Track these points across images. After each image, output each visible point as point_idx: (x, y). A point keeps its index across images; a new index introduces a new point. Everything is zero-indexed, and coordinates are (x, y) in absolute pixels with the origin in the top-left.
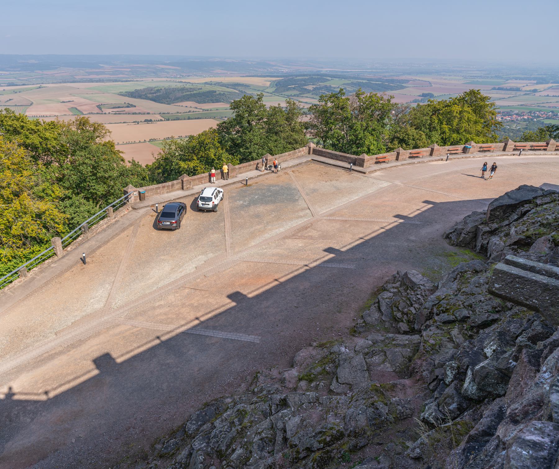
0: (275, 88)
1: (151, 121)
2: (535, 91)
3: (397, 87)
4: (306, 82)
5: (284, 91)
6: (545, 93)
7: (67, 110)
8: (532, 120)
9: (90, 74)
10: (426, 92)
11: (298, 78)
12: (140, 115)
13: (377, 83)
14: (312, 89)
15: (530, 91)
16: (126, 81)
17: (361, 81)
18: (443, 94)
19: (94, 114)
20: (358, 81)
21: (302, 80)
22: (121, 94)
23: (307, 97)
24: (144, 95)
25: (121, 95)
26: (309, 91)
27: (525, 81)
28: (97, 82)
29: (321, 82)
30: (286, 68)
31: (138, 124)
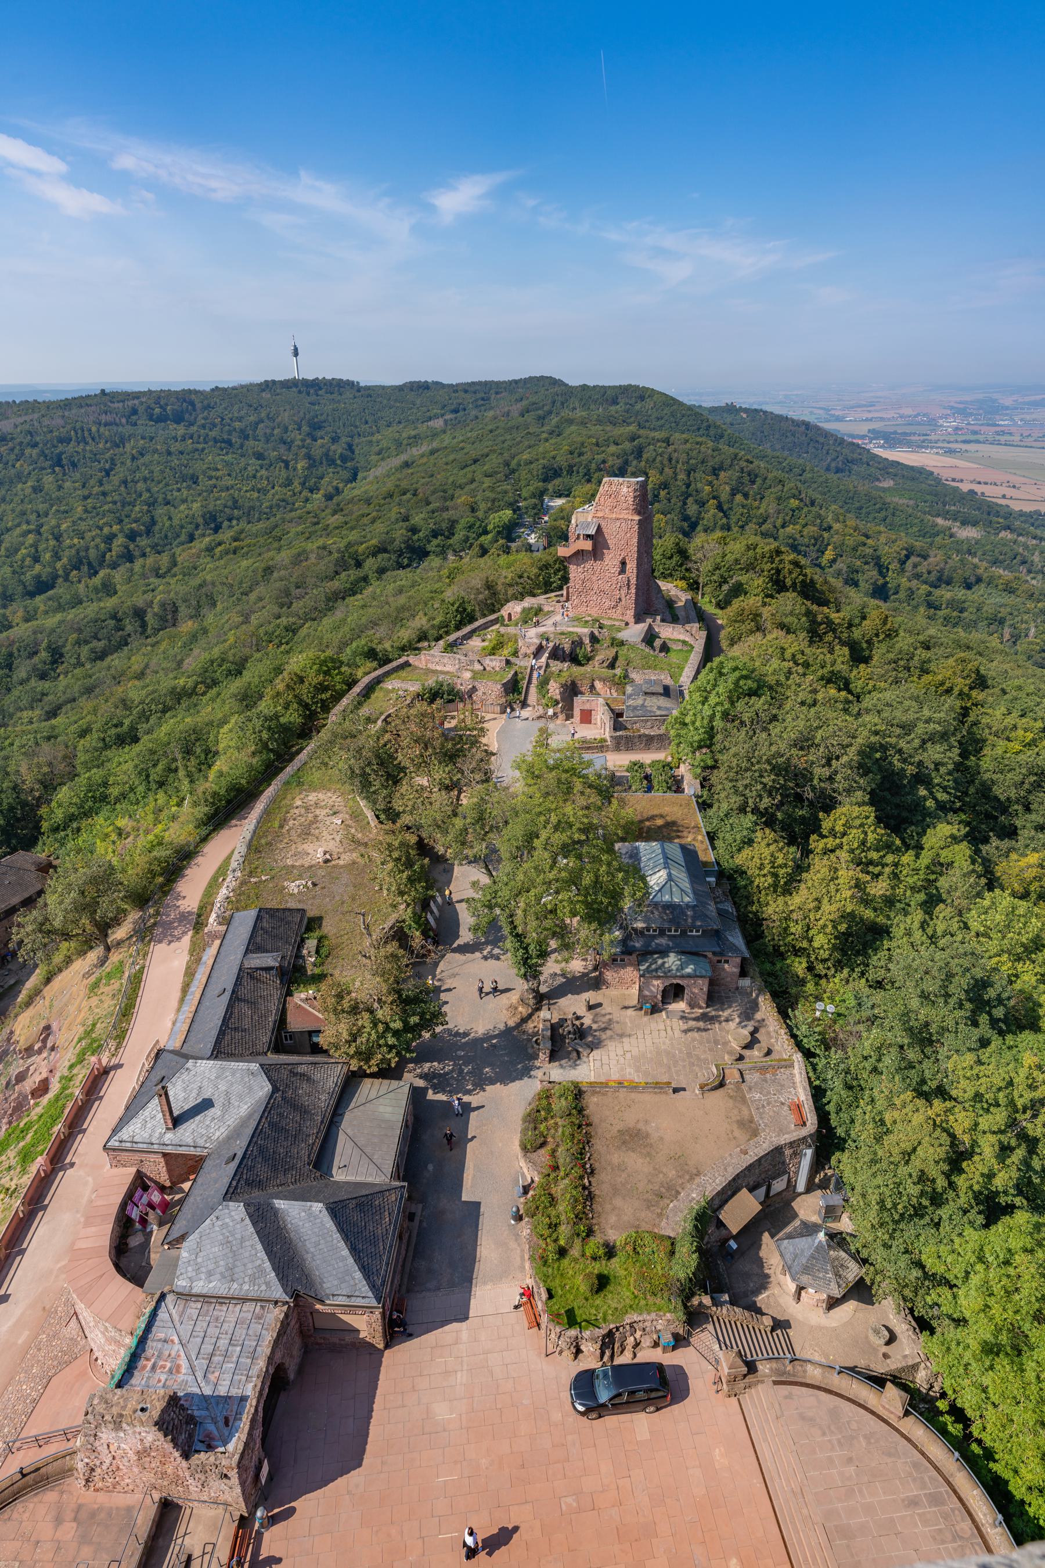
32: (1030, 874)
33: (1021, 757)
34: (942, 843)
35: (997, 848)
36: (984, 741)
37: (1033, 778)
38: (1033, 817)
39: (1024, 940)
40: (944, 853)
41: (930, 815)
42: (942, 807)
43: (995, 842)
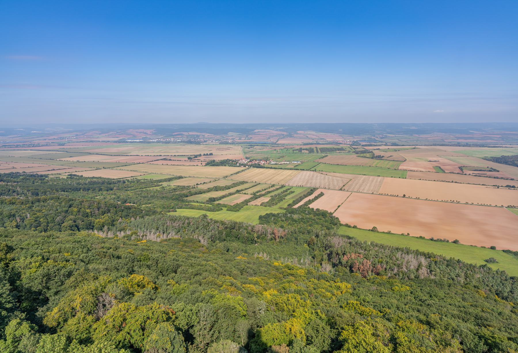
1: (514, 187)
7: (432, 167)
9: (458, 138)
12: (502, 180)
16: (494, 147)
19: (455, 173)
22: (486, 159)
24: (511, 162)
25: (485, 159)
28: (464, 146)
31: (498, 188)
32: (57, 316)
33: (38, 273)
34: (14, 329)
35: (42, 311)
36: (20, 272)
37: (45, 279)
38: (52, 291)
39: (62, 347)
40: (17, 333)
41: (6, 317)
42: (10, 310)
43: (40, 309)
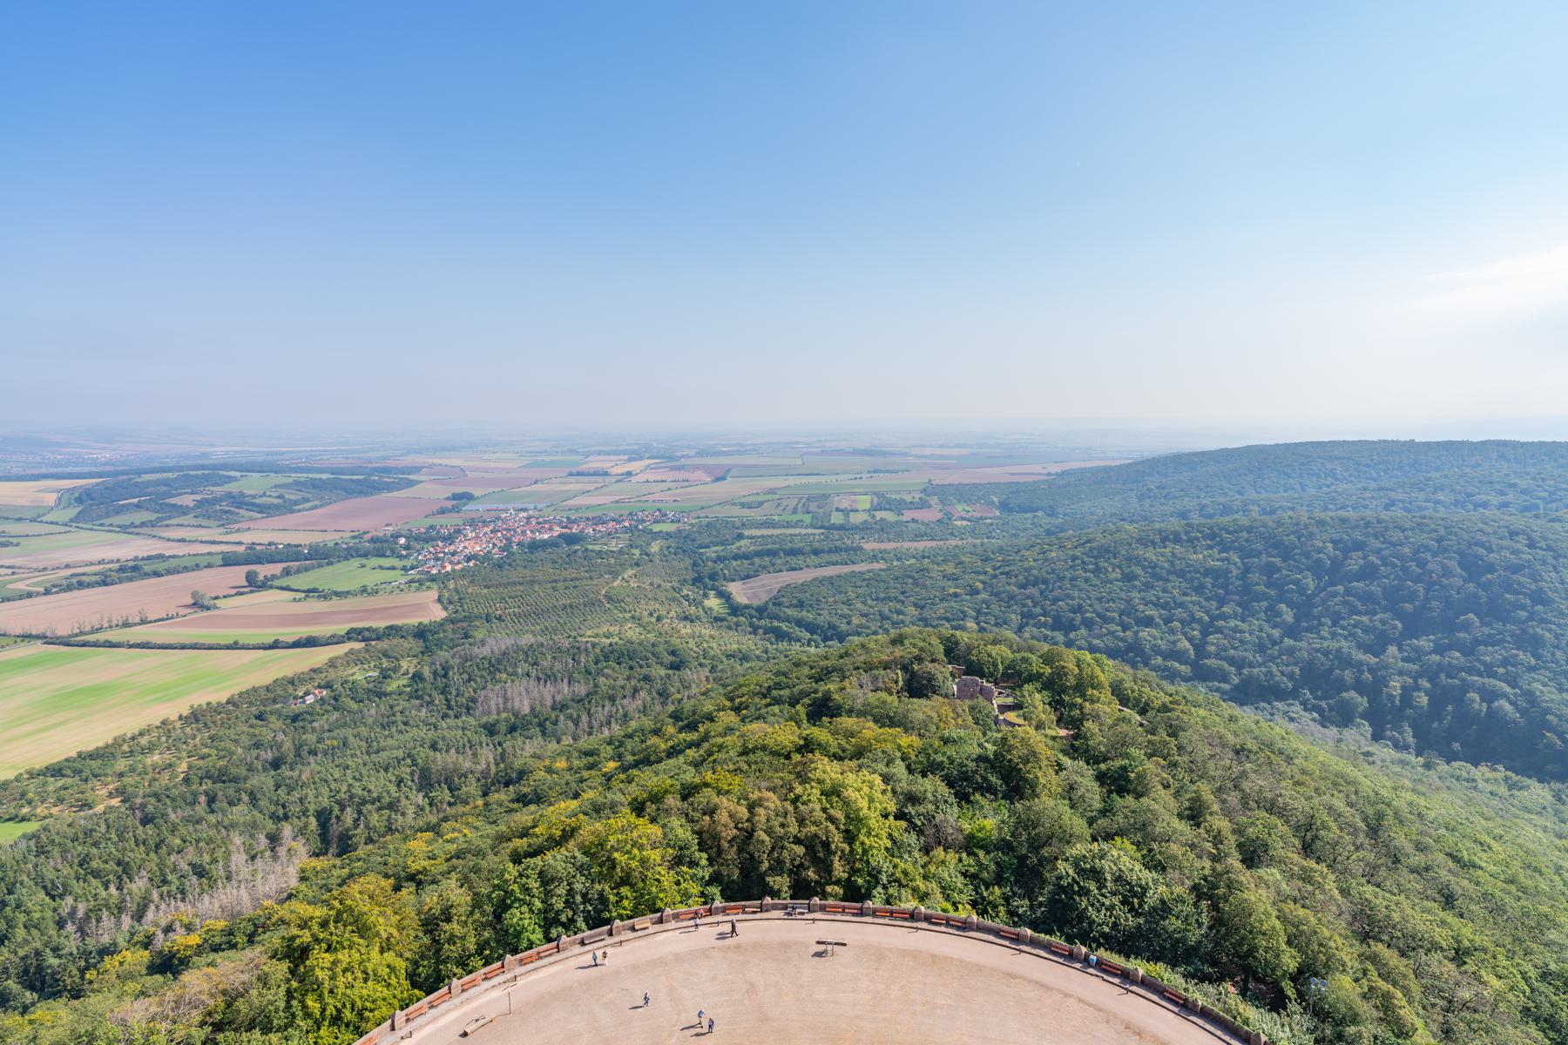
0: (78, 510)
2: (629, 474)
3: (398, 483)
4: (172, 487)
5: (108, 515)
6: (642, 477)
8: (636, 527)
10: (459, 490)
11: (146, 477)
13: (355, 477)
14: (191, 504)
15: (622, 475)
17: (317, 476)
18: (491, 490)
20: (311, 476)
21: (158, 483)
23: (181, 525)
26: (184, 511)
27: (612, 457)
29: (213, 485)
30: (104, 448)
